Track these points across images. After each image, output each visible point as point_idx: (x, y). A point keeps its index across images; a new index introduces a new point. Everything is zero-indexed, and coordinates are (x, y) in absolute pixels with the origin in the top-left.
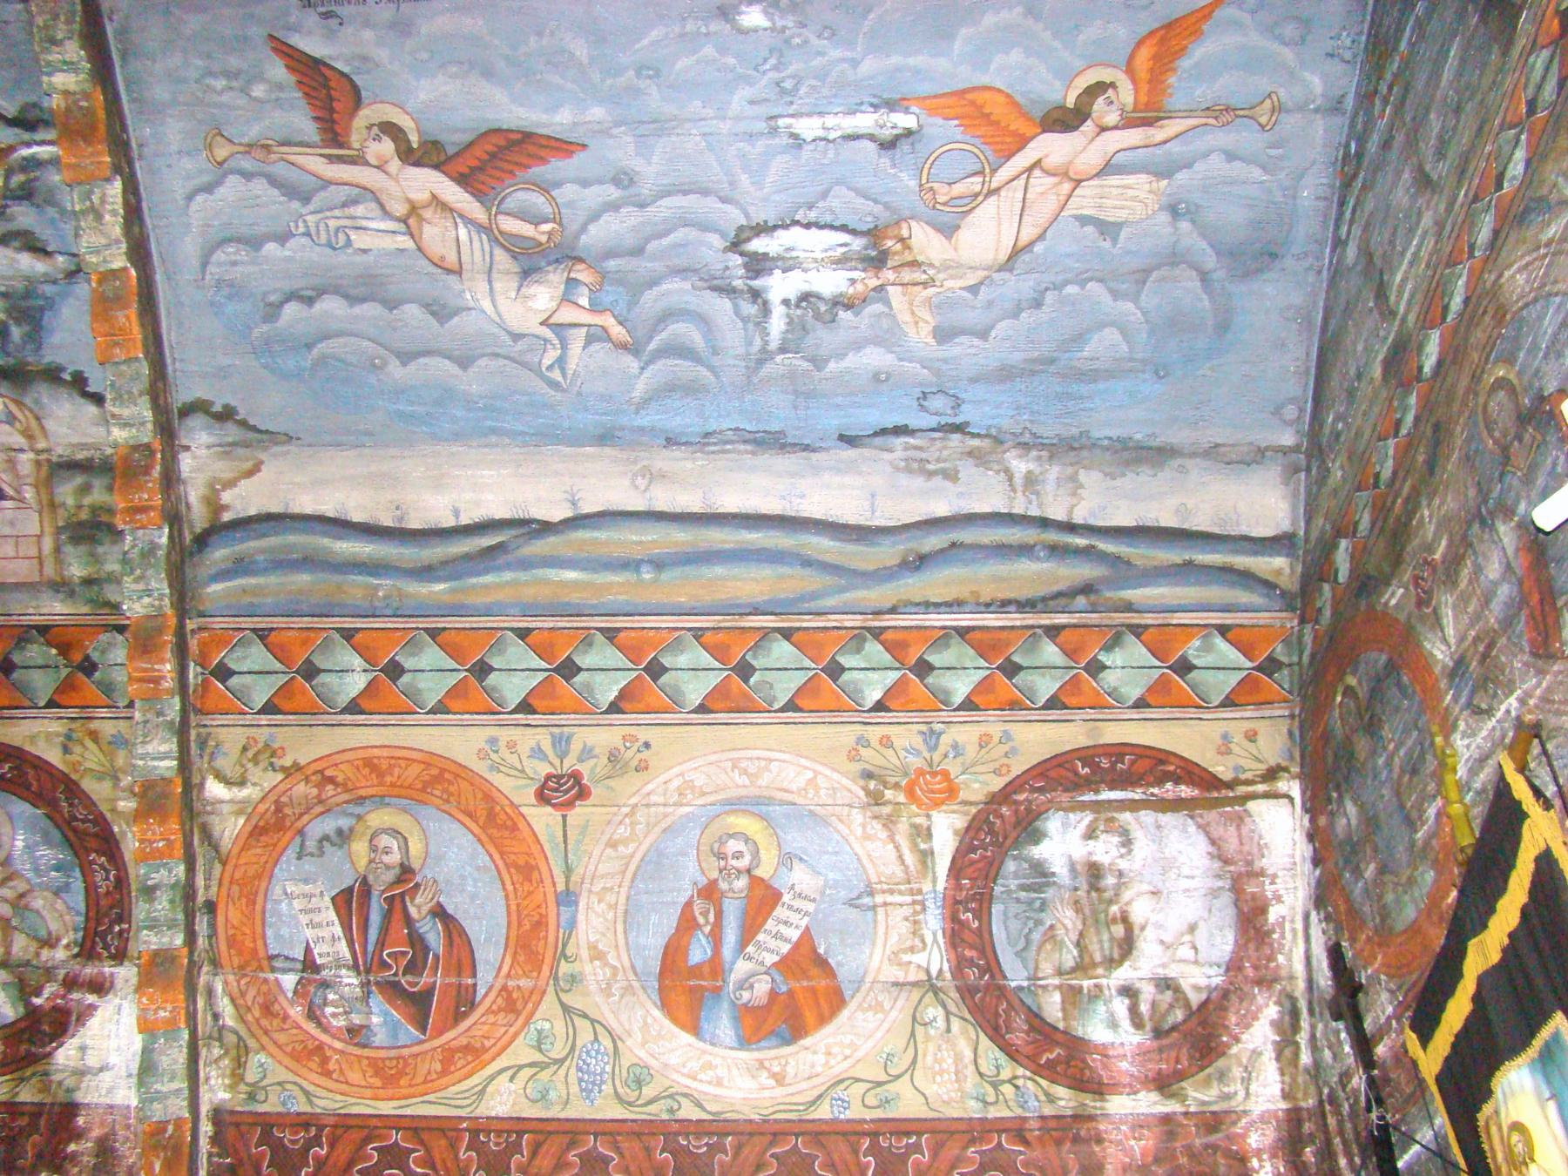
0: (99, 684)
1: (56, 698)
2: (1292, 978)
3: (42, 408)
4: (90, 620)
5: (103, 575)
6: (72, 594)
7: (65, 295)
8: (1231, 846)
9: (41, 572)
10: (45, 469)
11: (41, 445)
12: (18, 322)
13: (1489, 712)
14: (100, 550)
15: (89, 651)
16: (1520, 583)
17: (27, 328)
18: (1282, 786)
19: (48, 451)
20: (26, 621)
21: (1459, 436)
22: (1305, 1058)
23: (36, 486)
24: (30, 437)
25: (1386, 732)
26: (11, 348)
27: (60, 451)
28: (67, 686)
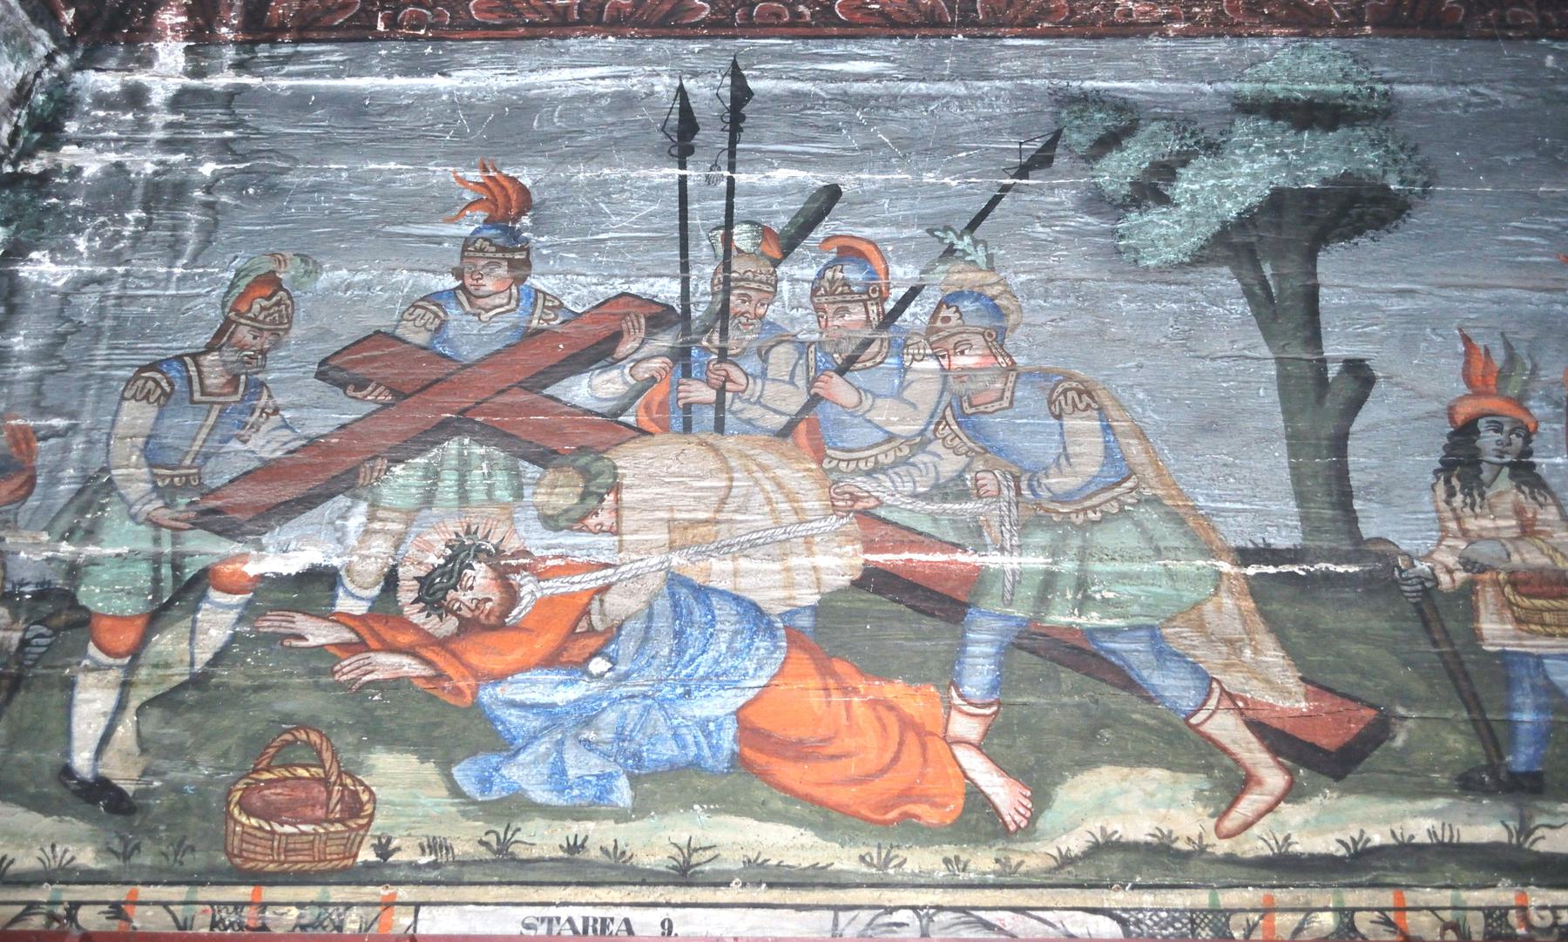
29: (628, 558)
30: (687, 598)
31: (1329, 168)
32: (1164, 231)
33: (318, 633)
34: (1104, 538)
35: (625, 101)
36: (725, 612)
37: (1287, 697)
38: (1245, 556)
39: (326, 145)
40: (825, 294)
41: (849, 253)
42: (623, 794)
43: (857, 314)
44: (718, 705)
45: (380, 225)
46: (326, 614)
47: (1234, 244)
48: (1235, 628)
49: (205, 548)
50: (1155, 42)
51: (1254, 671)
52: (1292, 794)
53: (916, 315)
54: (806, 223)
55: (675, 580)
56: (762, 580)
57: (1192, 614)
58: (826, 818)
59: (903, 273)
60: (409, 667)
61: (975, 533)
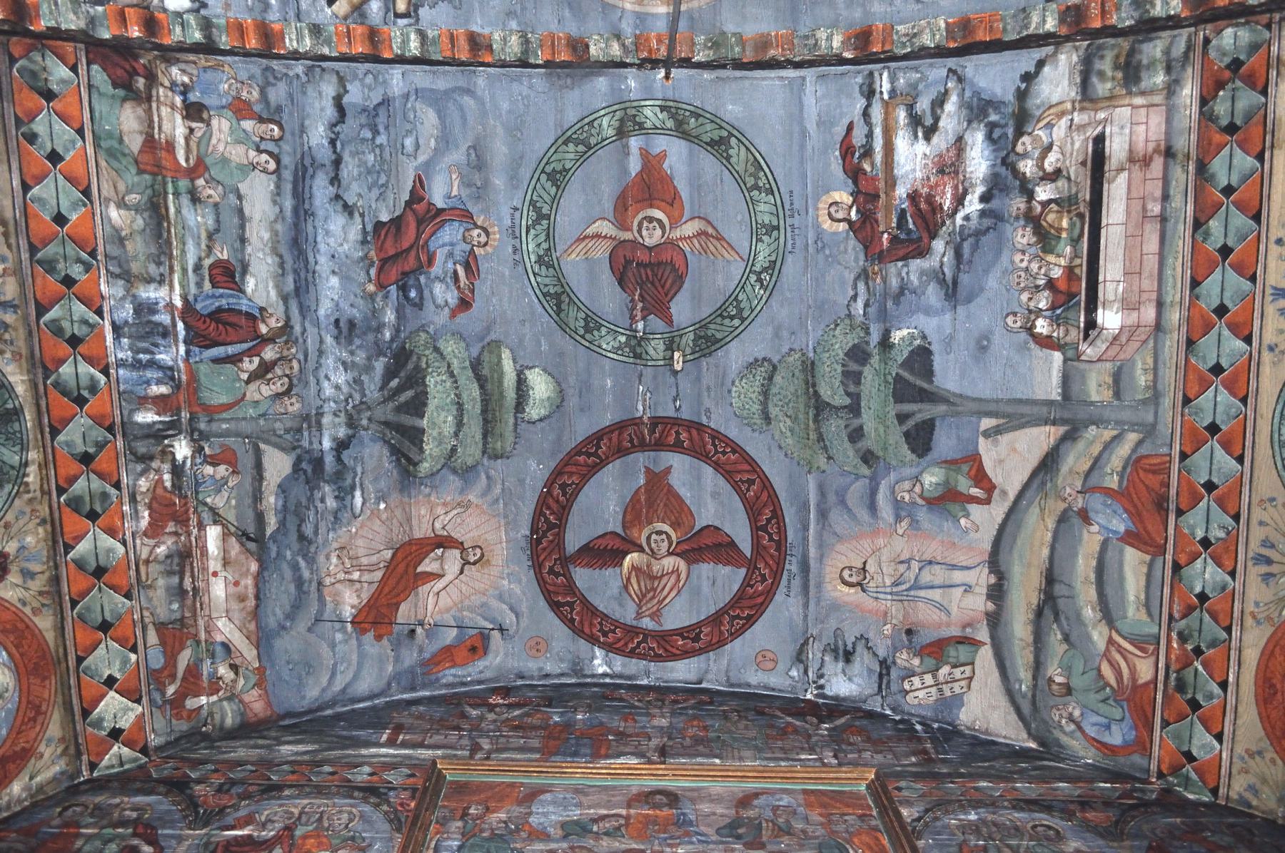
0: (1250, 55)
1: (1260, 88)
3: (1043, 103)
4: (1198, 66)
5: (1165, 58)
6: (1177, 82)
7: (972, 84)
9: (1157, 105)
10: (1086, 104)
11: (1069, 106)
12: (986, 116)
14: (1145, 62)
15: (1223, 65)
17: (991, 110)
19: (1073, 102)
20: (1195, 116)
23: (1096, 111)
24: (1063, 113)
26: (1003, 122)
27: (1073, 94)
28: (1250, 81)
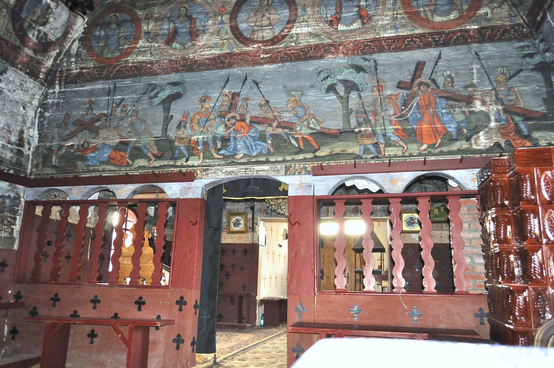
2: (65, 48)
8: (71, 20)
13: (150, 43)
16: (169, 33)
18: (85, 17)
21: (172, 6)
22: (58, 62)
25: (122, 29)
29: (98, 142)
30: (104, 145)
31: (176, 91)
32: (157, 100)
33: (72, 151)
34: (142, 137)
35: (104, 89)
36: (107, 146)
37: (156, 151)
38: (155, 138)
39: (74, 97)
40: (122, 111)
41: (124, 106)
42: (98, 164)
43: (124, 114)
44: (106, 155)
45: (78, 106)
46: (73, 148)
47: (163, 102)
48: (152, 145)
49: (63, 143)
50: (160, 76)
51: (153, 149)
52: (155, 161)
53: (130, 113)
54: (120, 103)
55: (103, 143)
56: (110, 142)
57: (149, 144)
58: (115, 165)
59: (129, 108)
60: (80, 153)
61: (130, 137)
